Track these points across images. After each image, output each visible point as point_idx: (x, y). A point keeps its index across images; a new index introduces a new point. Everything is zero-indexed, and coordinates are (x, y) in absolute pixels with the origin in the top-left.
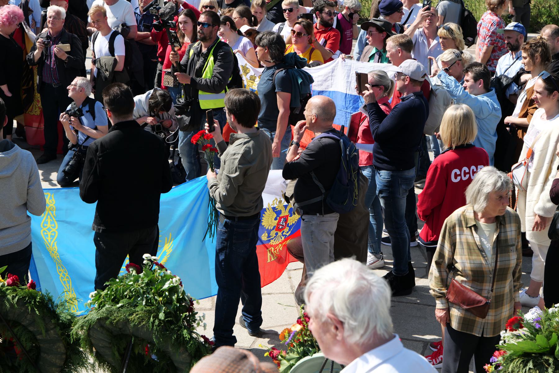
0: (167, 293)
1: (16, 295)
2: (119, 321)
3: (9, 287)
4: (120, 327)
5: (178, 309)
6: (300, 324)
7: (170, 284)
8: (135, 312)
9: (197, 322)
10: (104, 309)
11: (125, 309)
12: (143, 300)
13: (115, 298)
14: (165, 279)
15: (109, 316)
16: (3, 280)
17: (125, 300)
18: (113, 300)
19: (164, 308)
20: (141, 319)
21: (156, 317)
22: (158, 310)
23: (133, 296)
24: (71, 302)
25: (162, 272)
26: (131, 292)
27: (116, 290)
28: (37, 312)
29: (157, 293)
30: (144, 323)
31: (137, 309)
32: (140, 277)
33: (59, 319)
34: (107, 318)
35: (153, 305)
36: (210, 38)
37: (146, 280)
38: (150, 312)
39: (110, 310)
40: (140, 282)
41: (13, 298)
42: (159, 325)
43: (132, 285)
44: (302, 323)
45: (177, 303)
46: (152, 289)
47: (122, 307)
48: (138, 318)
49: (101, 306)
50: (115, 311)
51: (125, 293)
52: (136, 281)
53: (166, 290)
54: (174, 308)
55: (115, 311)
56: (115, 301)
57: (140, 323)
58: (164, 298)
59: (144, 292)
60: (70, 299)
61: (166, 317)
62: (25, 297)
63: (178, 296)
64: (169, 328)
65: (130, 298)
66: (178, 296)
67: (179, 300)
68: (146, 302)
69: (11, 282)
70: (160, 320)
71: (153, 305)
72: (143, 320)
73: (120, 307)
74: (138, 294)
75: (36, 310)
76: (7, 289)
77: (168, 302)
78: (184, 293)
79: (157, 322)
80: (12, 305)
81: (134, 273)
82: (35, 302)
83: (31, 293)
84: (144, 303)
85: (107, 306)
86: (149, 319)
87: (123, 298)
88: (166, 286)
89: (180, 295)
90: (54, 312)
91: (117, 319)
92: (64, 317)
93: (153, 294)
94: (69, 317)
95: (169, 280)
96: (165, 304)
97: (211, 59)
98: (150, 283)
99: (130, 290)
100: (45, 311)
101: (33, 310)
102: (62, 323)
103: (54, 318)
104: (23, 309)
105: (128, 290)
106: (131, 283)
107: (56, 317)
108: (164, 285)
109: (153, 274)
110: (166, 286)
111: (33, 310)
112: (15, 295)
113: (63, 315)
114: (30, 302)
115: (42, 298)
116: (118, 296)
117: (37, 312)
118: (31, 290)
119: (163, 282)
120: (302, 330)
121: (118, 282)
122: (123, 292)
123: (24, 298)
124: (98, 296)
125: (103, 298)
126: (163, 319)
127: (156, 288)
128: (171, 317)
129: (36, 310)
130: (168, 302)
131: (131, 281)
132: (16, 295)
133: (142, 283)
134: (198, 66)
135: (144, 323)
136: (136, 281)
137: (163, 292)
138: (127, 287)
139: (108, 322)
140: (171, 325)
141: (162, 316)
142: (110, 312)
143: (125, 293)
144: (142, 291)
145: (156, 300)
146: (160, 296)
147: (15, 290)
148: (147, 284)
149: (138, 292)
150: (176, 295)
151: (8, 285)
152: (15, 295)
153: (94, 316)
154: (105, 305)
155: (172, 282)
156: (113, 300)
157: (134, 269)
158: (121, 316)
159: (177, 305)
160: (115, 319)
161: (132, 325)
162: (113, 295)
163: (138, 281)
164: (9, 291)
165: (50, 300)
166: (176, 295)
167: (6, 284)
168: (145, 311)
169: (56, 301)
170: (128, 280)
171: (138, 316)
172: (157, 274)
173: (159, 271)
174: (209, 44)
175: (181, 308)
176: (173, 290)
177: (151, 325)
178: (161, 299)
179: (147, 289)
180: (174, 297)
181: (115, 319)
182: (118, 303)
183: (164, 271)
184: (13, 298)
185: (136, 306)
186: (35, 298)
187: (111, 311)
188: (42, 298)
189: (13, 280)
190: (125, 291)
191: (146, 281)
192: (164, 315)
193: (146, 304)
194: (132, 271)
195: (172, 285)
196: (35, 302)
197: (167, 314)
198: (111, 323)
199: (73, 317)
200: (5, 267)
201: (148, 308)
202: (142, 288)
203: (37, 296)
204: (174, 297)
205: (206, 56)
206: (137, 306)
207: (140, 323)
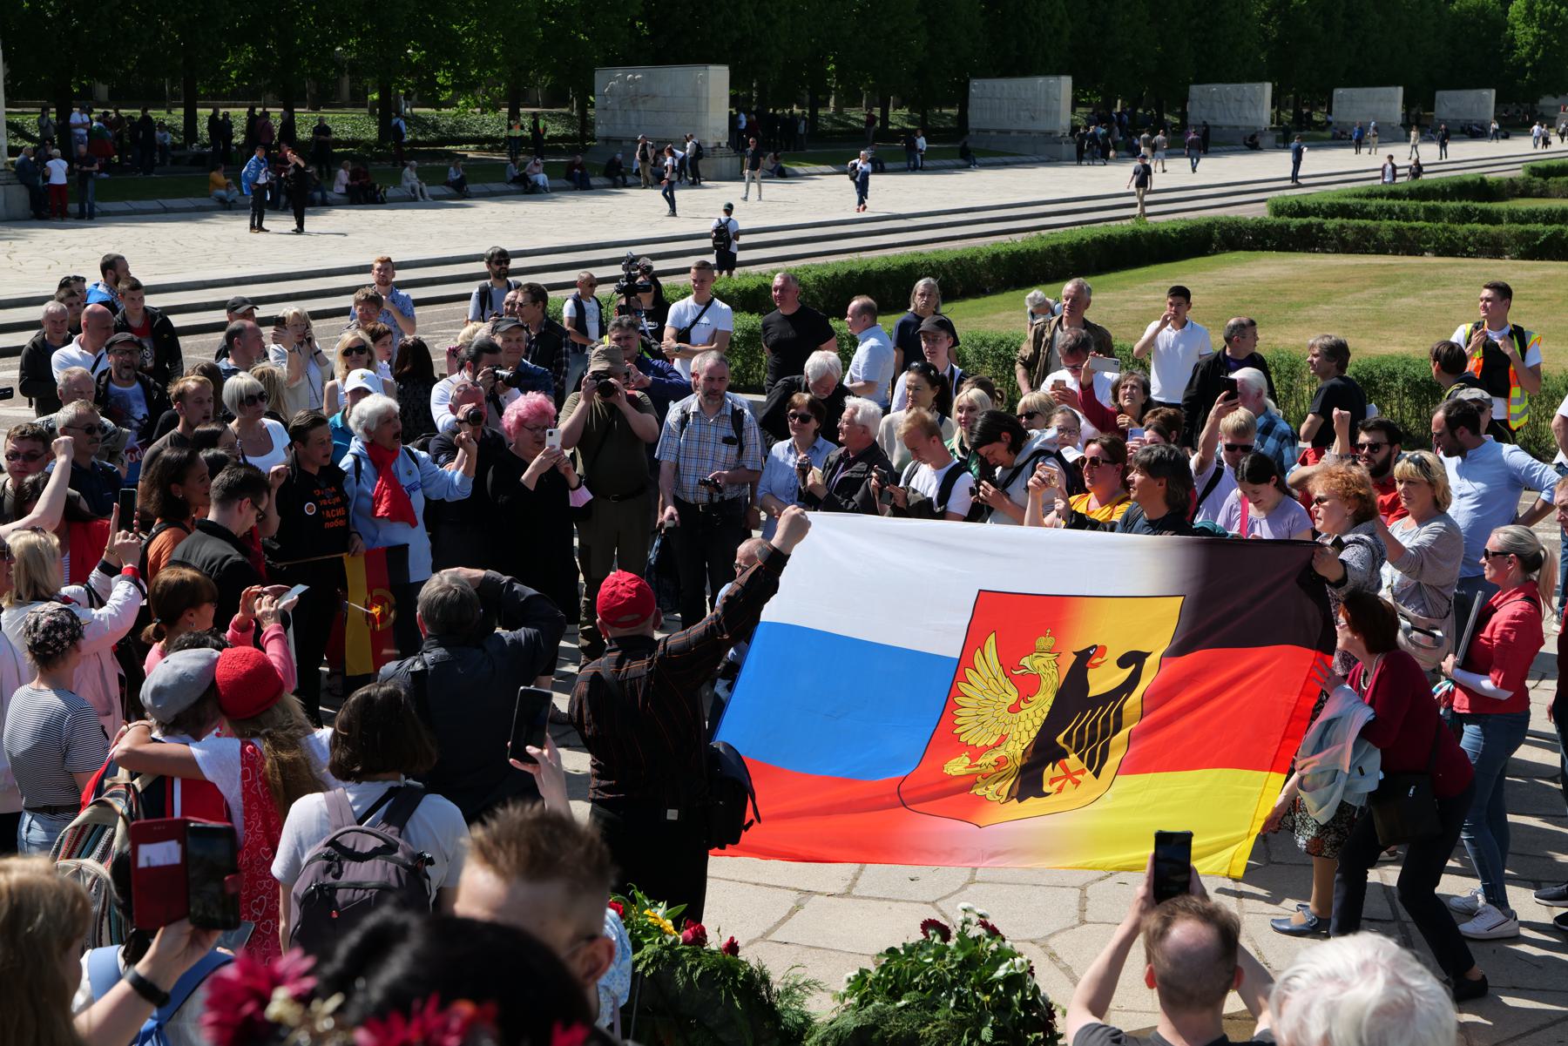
2: (898, 1035)
8: (932, 1020)
10: (870, 1008)
11: (913, 1013)
14: (1001, 956)
17: (913, 994)
18: (890, 993)
21: (975, 1035)
22: (981, 1021)
23: (930, 986)
26: (927, 978)
27: (898, 972)
28: (738, 1004)
32: (948, 948)
34: (873, 1028)
35: (970, 1009)
38: (962, 1024)
47: (906, 1007)
48: (938, 1034)
49: (864, 1001)
52: (940, 956)
53: (999, 981)
56: (895, 995)
58: (993, 997)
61: (995, 1038)
62: (716, 970)
63: (1024, 995)
65: (924, 991)
66: (1024, 995)
67: (1024, 1004)
74: (941, 985)
76: (682, 951)
77: (1002, 1006)
78: (1036, 990)
81: (937, 940)
82: (735, 980)
83: (728, 963)
85: (877, 1003)
87: (909, 990)
88: (1001, 972)
90: (772, 1005)
94: (800, 1020)
98: (970, 963)
101: (728, 996)
107: (772, 1014)
110: (1001, 972)
113: (788, 1014)
114: (725, 982)
117: (738, 1004)
118: (728, 956)
122: (912, 977)
123: (713, 971)
127: (979, 975)
130: (1002, 1006)
131: (929, 955)
133: (952, 962)
136: (940, 956)
138: (921, 968)
139: (875, 1036)
141: (986, 1033)
142: (882, 1016)
144: (949, 977)
145: (977, 1000)
146: (985, 993)
148: (962, 965)
153: (851, 1022)
154: (871, 1001)
155: (1013, 965)
156: (890, 993)
163: (943, 957)
165: (765, 979)
169: (778, 982)
172: (982, 946)
176: (1015, 981)
179: (961, 975)
180: (1016, 998)
184: (694, 968)
185: (935, 1008)
186: (736, 973)
188: (750, 975)
189: (695, 934)
198: (882, 1039)
199: (808, 1021)
200: (683, 907)
201: (960, 1015)
202: (950, 971)
204: (1016, 998)
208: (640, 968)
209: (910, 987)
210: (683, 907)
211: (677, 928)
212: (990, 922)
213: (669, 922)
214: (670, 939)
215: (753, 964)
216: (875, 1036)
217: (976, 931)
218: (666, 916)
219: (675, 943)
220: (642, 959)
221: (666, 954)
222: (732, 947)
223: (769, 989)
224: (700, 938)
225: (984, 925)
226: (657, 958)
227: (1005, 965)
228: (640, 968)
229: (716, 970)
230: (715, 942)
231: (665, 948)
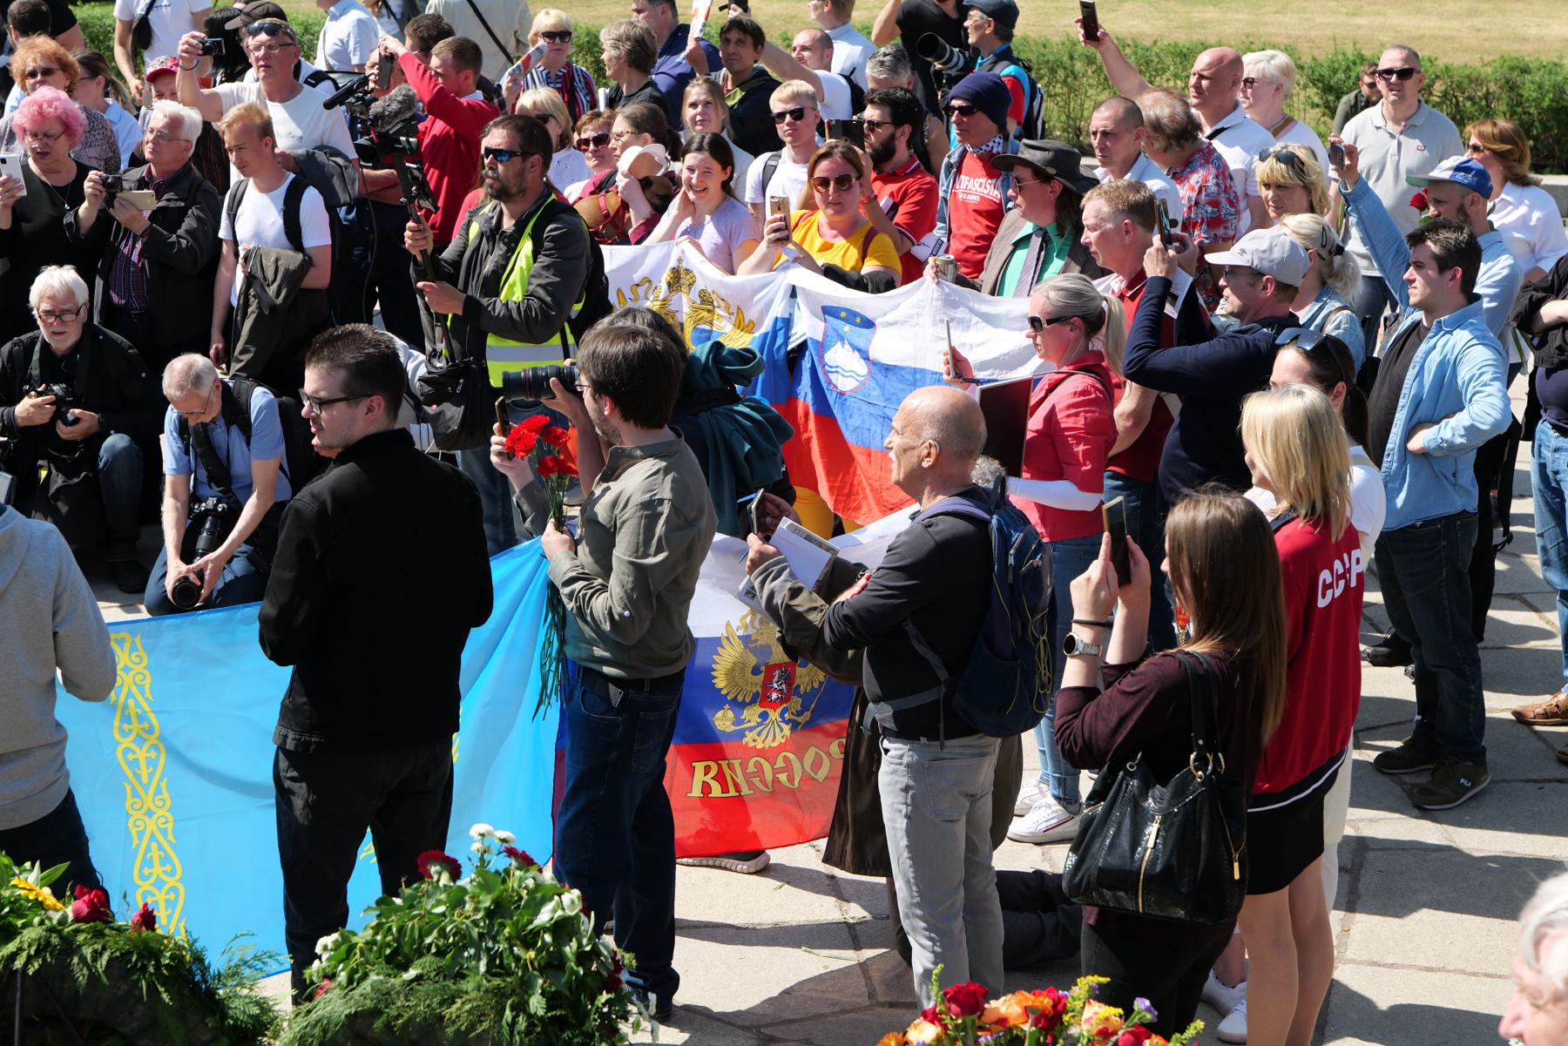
0: (548, 938)
1: (104, 948)
2: (410, 1019)
3: (83, 926)
4: (414, 1037)
5: (581, 981)
6: (932, 1022)
7: (554, 911)
8: (460, 993)
9: (631, 1020)
10: (366, 986)
11: (426, 986)
12: (479, 960)
13: (396, 952)
15: (382, 1006)
16: (59, 905)
17: (428, 959)
19: (540, 981)
20: (478, 1015)
21: (521, 1007)
22: (526, 986)
23: (448, 946)
24: (260, 965)
25: (529, 874)
26: (443, 934)
27: (401, 929)
28: (165, 996)
29: (518, 937)
30: (485, 1025)
31: (468, 985)
32: (463, 890)
33: (224, 1016)
34: (375, 1013)
35: (509, 973)
36: (522, 191)
37: (487, 902)
38: (500, 995)
39: (384, 988)
40: (469, 907)
41: (97, 955)
42: (528, 1032)
43: (443, 915)
44: (940, 1020)
45: (578, 964)
46: (503, 926)
47: (419, 978)
48: (469, 1012)
50: (398, 993)
51: (428, 940)
52: (457, 902)
53: (545, 929)
54: (569, 981)
55: (398, 993)
56: (398, 960)
57: (472, 1027)
58: (539, 952)
59: (481, 935)
60: (255, 957)
61: (549, 1008)
62: (130, 953)
63: (580, 945)
64: (558, 1037)
65: (440, 953)
66: (580, 945)
67: (582, 958)
68: (488, 964)
69: (86, 910)
70: (530, 1016)
71: (509, 973)
72: (482, 1016)
73: (412, 981)
74: (464, 939)
75: (162, 989)
76: (77, 931)
77: (553, 965)
79: (522, 1023)
80: (93, 978)
81: (445, 879)
82: (158, 966)
83: (145, 943)
84: (483, 968)
85: (373, 977)
86: (501, 1013)
87: (420, 955)
88: (545, 916)
89: (585, 941)
90: (211, 993)
91: (406, 1016)
92: (240, 1007)
93: (508, 939)
94: (256, 1011)
95: (551, 899)
96: (542, 970)
97: (526, 246)
99: (443, 929)
100: (186, 992)
101: (152, 989)
102: (235, 1026)
103: (212, 1012)
104: (124, 987)
105: (435, 933)
106: (441, 909)
107: (217, 1007)
108: (536, 913)
109: (504, 881)
110: (545, 916)
111: (152, 989)
112: (98, 947)
114: (144, 968)
115: (177, 958)
116: (406, 950)
117: (165, 996)
118: (145, 933)
119: (536, 905)
120: (938, 1039)
121: (399, 909)
123: (126, 955)
124: (344, 948)
125: (362, 955)
126: (541, 1012)
127: (515, 924)
128: (561, 1007)
129: (162, 989)
130: (553, 965)
131: (439, 903)
132: (104, 948)
133: (476, 910)
134: (488, 267)
135: (485, 1025)
136: (457, 902)
137: (536, 934)
139: (378, 1024)
140: (563, 1031)
141: (537, 1004)
142: (385, 996)
143: (428, 940)
144: (475, 932)
145: (518, 959)
147: (98, 934)
148: (490, 914)
149: (464, 937)
150: (574, 944)
151: (77, 919)
152: (98, 947)
154: (365, 976)
155: (561, 905)
156: (389, 960)
157: (443, 868)
158: (418, 1006)
159: (577, 973)
160: (399, 1016)
161: (450, 1031)
162: (389, 945)
163: (462, 903)
164: (81, 938)
165: (199, 959)
166: (574, 944)
167: (71, 917)
168: (487, 991)
169: (216, 962)
170: (432, 902)
171: (468, 1007)
172: (513, 883)
173: (518, 873)
174: (523, 206)
175: (589, 980)
177: (506, 1030)
178: (532, 954)
179: (491, 926)
180: (570, 949)
181: (399, 1016)
182: (406, 968)
183: (533, 872)
184: (97, 955)
185: (461, 976)
186: (156, 955)
187: (388, 993)
188: (177, 958)
189: (90, 904)
190: (429, 933)
191: (487, 904)
192: (543, 1001)
193: (488, 971)
194: (440, 874)
195: (560, 913)
196: (158, 966)
197: (552, 1000)
198: (388, 1027)
200: (63, 866)
201: (496, 981)
202: (475, 923)
203: (161, 952)
204: (570, 949)
205: (513, 242)
206: (463, 977)
207: (472, 1027)
208: (19, 964)
209: (421, 952)
210: (63, 866)
211: (58, 893)
212: (520, 848)
213: (47, 891)
214: (56, 917)
215: (181, 938)
216: (378, 1024)
217: (499, 862)
218: (43, 882)
219: (63, 921)
220: (20, 949)
221: (55, 940)
222: (148, 918)
223: (205, 970)
224: (100, 912)
225: (511, 852)
226: (43, 947)
227: (549, 906)
228: (19, 964)
229: (130, 953)
230: (125, 915)
231: (51, 930)
